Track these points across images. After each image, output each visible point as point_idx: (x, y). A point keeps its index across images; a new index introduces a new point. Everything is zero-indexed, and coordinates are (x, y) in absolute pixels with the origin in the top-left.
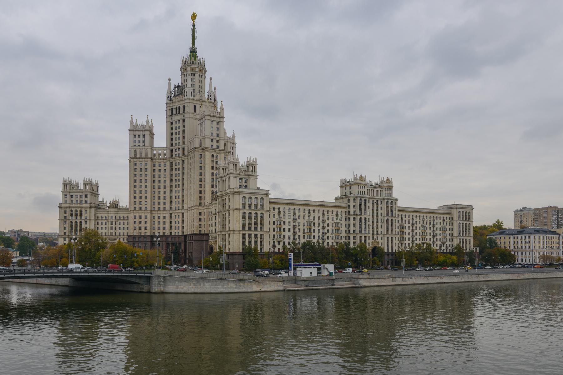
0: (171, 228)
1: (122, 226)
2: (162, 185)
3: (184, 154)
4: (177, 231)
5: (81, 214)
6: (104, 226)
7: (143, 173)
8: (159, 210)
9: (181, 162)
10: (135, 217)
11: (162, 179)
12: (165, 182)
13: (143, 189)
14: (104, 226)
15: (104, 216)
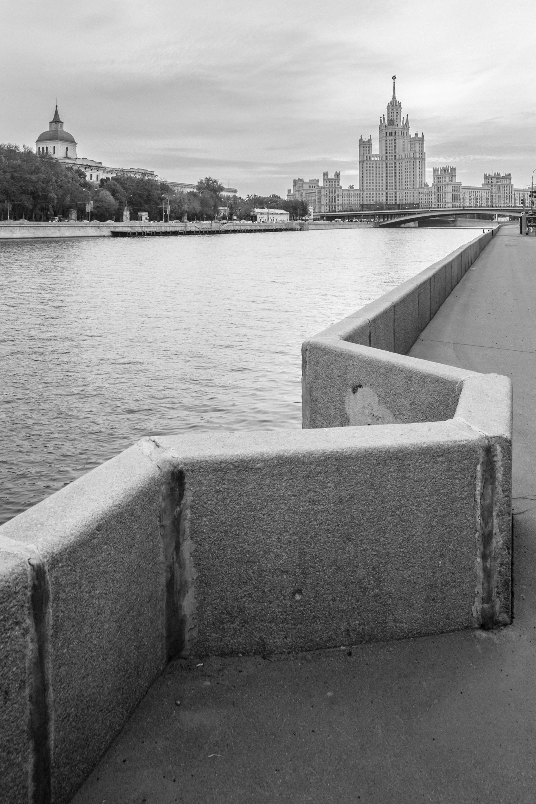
0: (387, 200)
1: (356, 199)
2: (381, 175)
3: (395, 158)
4: (391, 202)
5: (335, 192)
6: (346, 199)
7: (371, 169)
8: (379, 189)
9: (394, 164)
10: (367, 194)
11: (381, 172)
12: (382, 174)
13: (371, 178)
14: (346, 199)
15: (346, 193)
